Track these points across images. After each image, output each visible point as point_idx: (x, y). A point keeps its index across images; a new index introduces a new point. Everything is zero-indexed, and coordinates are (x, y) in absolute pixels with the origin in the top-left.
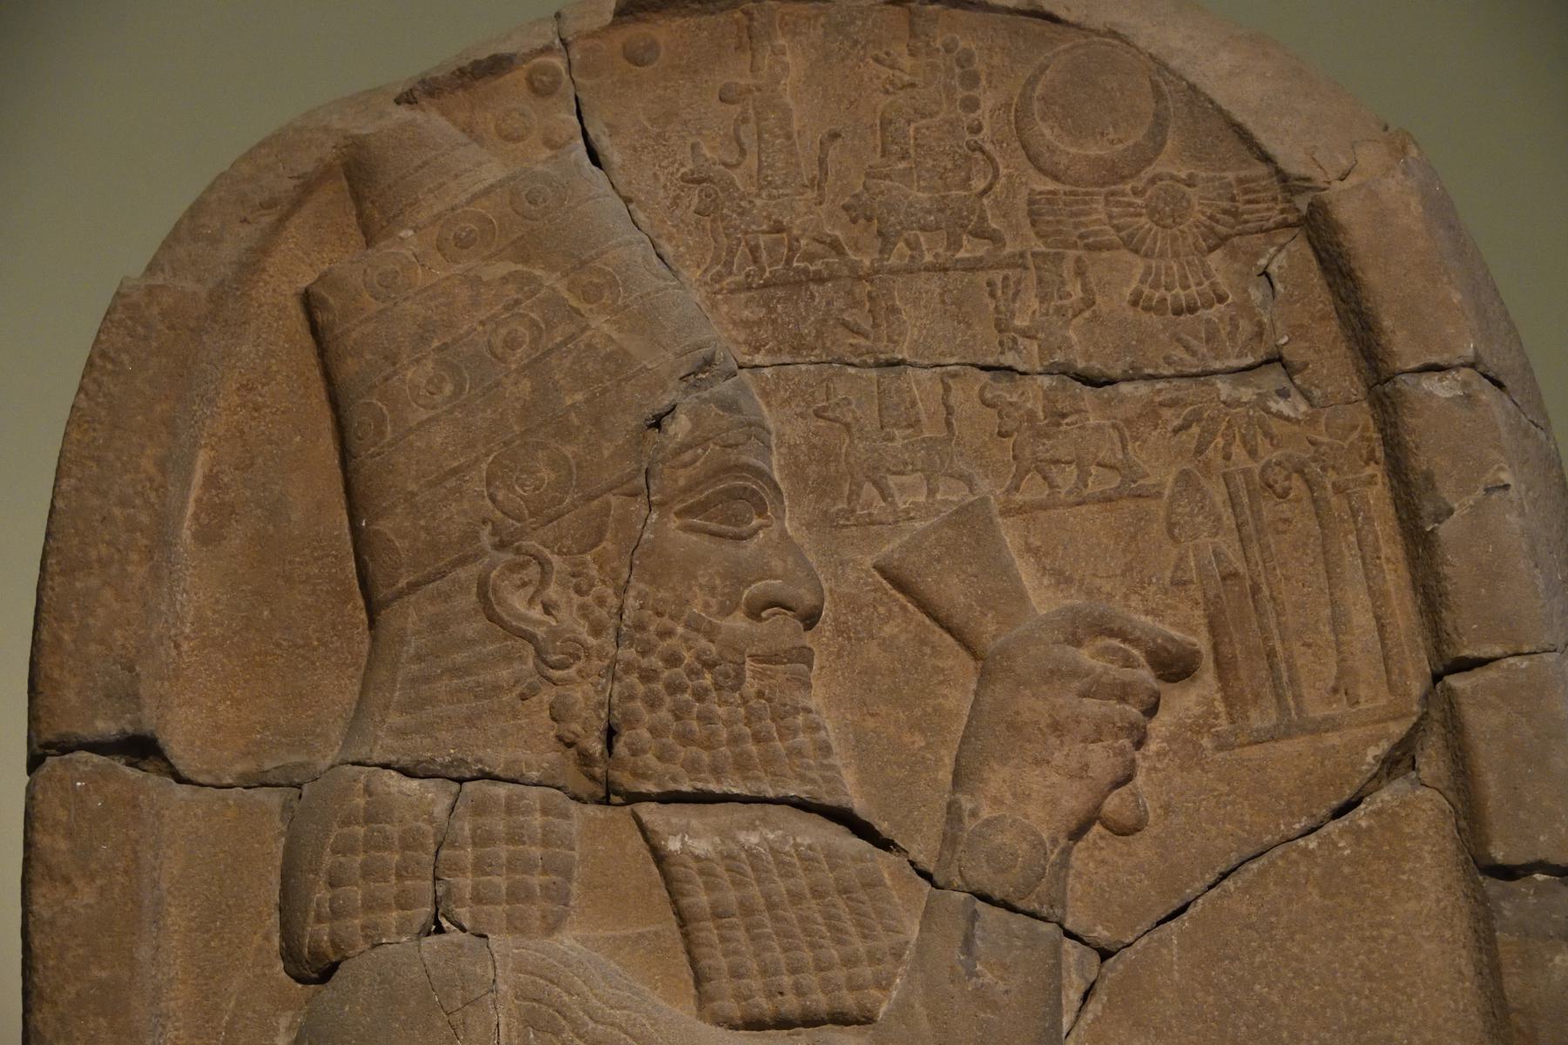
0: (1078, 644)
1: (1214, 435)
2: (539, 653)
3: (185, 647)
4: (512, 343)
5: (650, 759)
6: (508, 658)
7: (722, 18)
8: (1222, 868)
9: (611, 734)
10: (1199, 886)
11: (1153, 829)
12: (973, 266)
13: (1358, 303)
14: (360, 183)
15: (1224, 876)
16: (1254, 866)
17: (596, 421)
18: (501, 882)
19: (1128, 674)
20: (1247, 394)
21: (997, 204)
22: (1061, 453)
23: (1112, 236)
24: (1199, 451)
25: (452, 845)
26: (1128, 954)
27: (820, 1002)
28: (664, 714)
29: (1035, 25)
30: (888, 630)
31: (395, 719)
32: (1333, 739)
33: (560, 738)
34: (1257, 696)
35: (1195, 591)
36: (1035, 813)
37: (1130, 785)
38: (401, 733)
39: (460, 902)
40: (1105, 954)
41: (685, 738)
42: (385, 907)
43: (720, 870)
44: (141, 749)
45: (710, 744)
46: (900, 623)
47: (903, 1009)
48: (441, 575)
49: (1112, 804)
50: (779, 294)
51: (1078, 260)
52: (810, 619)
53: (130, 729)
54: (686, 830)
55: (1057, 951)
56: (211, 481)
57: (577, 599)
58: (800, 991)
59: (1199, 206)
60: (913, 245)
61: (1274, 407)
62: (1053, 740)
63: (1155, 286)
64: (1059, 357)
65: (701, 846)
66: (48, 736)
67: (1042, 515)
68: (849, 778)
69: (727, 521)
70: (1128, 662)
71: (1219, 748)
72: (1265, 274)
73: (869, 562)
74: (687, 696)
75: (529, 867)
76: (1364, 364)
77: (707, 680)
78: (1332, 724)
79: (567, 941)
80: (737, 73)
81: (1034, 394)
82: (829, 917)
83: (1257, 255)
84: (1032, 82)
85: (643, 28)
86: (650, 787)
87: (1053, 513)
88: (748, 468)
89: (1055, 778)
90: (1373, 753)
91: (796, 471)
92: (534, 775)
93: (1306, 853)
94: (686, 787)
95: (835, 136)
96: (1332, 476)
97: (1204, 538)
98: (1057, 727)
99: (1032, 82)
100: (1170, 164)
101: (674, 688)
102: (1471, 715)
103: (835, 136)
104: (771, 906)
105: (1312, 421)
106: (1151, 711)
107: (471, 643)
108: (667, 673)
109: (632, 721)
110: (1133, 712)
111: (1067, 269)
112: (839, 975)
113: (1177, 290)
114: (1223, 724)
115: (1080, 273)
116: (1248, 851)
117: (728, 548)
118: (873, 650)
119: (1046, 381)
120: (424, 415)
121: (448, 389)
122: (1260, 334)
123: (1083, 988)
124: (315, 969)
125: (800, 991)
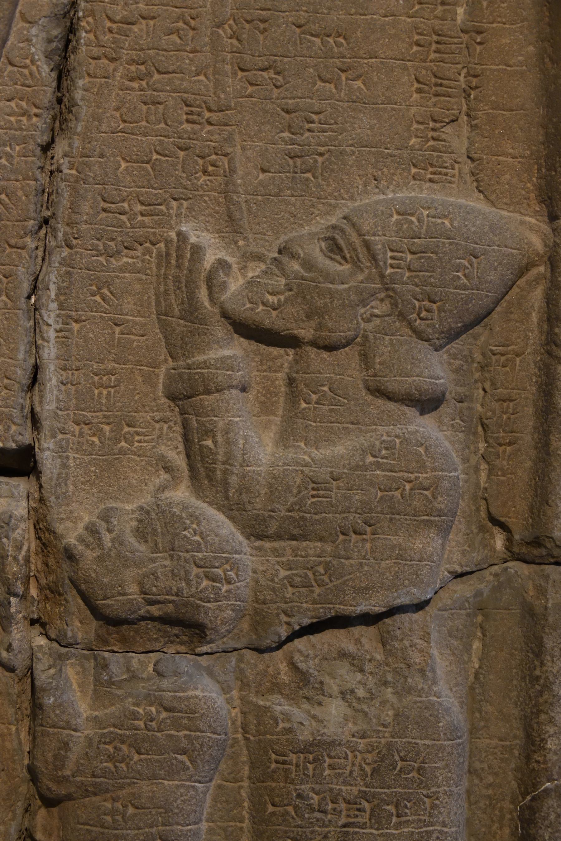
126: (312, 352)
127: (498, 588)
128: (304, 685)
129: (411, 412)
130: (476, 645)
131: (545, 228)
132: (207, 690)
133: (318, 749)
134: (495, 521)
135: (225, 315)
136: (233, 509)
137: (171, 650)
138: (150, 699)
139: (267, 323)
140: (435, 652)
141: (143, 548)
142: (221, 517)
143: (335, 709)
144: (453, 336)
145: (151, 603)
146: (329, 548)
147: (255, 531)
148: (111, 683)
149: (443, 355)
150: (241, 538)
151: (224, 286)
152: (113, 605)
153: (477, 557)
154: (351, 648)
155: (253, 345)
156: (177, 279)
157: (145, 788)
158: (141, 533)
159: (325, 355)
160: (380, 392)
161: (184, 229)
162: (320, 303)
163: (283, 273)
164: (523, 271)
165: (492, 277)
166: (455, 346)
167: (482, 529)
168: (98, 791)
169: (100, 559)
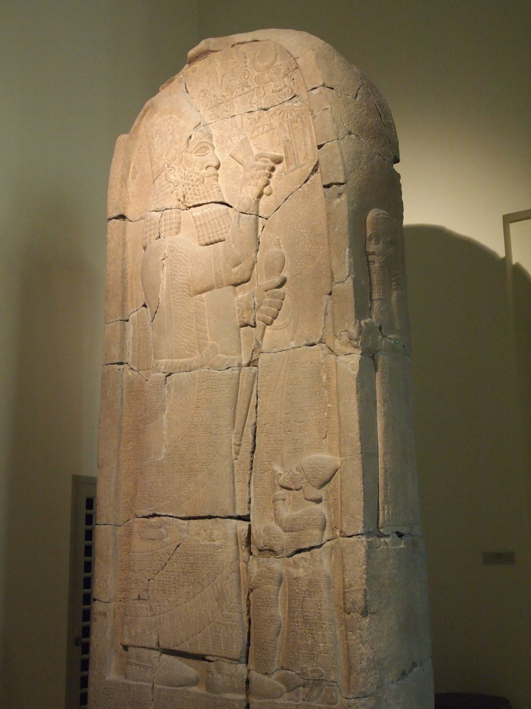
0: (257, 160)
1: (285, 114)
3: (130, 198)
4: (169, 130)
5: (190, 200)
6: (169, 187)
7: (206, 59)
8: (285, 198)
9: (184, 196)
10: (282, 202)
15: (286, 199)
16: (291, 196)
17: (181, 140)
18: (168, 227)
19: (265, 164)
20: (290, 104)
21: (250, 80)
22: (260, 125)
26: (270, 218)
27: (217, 238)
28: (192, 191)
31: (155, 202)
32: (304, 168)
34: (292, 163)
35: (281, 145)
36: (250, 195)
37: (268, 186)
38: (155, 204)
40: (267, 219)
41: (195, 195)
43: (201, 217)
44: (122, 217)
48: (160, 175)
49: (266, 190)
50: (215, 108)
51: (263, 86)
52: (217, 168)
53: (119, 214)
54: (197, 212)
55: (257, 219)
56: (134, 167)
59: (283, 69)
60: (237, 92)
61: (294, 105)
62: (251, 180)
64: (260, 107)
65: (198, 214)
66: (108, 218)
67: (257, 138)
68: (225, 196)
69: (201, 153)
70: (266, 162)
73: (228, 154)
75: (172, 224)
77: (198, 182)
78: (304, 165)
81: (255, 115)
82: (218, 222)
85: (194, 65)
87: (259, 137)
88: (204, 142)
89: (252, 187)
91: (217, 141)
92: (174, 207)
93: (299, 191)
94: (196, 203)
97: (283, 134)
100: (278, 63)
101: (193, 186)
103: (224, 76)
104: (209, 222)
105: (301, 106)
106: (273, 169)
107: (164, 186)
108: (191, 183)
109: (187, 193)
110: (267, 171)
111: (261, 88)
113: (279, 87)
116: (290, 193)
117: (202, 158)
119: (258, 112)
120: (157, 146)
121: (160, 141)
122: (292, 91)
123: (262, 226)
127: (336, 543)
128: (296, 565)
129: (313, 503)
130: (333, 557)
132: (277, 565)
133: (297, 579)
136: (280, 526)
137: (272, 557)
138: (266, 567)
140: (324, 558)
141: (263, 534)
142: (278, 527)
143: (301, 570)
144: (321, 486)
145: (266, 546)
146: (297, 533)
149: (321, 490)
150: (282, 531)
151: (279, 478)
153: (331, 536)
154: (305, 557)
158: (264, 531)
159: (297, 492)
160: (306, 499)
164: (337, 470)
165: (328, 472)
166: (324, 488)
167: (333, 529)
169: (257, 537)
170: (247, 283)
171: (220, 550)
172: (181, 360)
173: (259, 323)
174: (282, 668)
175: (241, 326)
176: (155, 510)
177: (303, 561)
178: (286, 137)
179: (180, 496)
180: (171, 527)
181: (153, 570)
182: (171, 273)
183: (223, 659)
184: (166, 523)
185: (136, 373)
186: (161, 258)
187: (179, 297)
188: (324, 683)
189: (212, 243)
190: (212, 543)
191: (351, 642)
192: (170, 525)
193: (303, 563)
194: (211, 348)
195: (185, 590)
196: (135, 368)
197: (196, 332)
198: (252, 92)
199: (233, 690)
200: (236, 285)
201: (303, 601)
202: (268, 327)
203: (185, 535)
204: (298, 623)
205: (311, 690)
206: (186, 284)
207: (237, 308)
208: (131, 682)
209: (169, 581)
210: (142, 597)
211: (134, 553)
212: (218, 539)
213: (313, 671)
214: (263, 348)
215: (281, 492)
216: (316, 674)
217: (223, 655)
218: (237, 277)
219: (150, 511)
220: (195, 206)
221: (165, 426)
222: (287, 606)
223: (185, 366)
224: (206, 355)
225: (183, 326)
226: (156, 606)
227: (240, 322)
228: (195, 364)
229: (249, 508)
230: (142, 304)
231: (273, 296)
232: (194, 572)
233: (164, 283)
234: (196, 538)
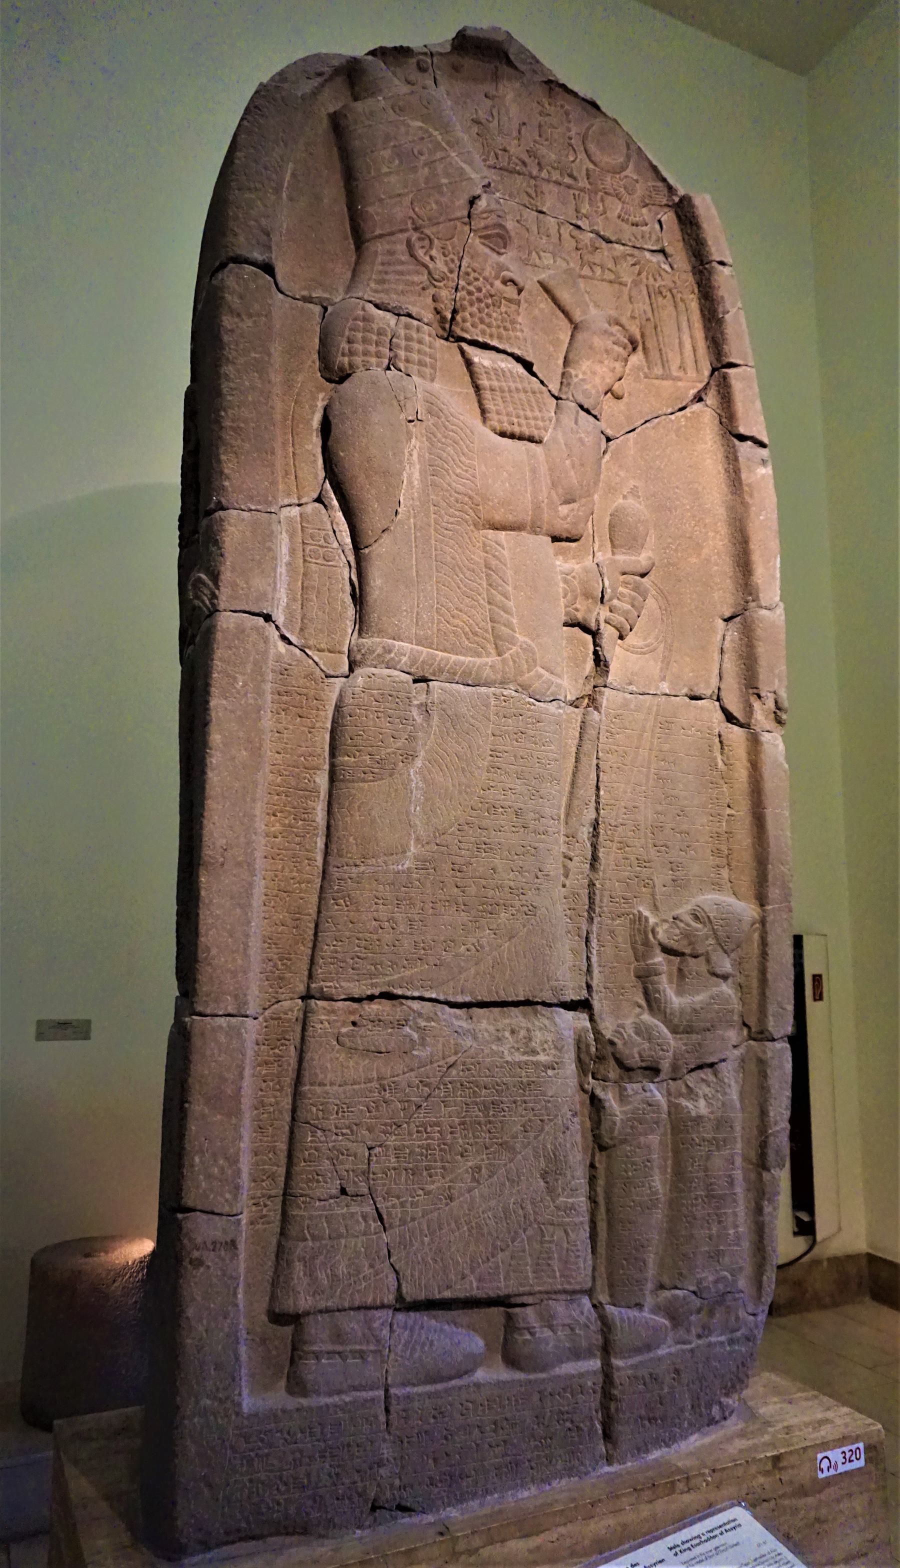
2: (430, 273)
5: (468, 324)
9: (455, 312)
11: (625, 400)
12: (569, 187)
13: (698, 235)
14: (352, 74)
22: (597, 261)
23: (612, 191)
24: (639, 274)
25: (398, 338)
26: (617, 441)
28: (474, 309)
29: (589, 107)
30: (542, 306)
32: (680, 384)
33: (436, 309)
35: (637, 322)
39: (400, 360)
40: (609, 440)
41: (482, 321)
42: (371, 356)
45: (489, 326)
46: (545, 304)
47: (554, 440)
52: (520, 291)
57: (443, 258)
58: (519, 425)
62: (605, 356)
63: (626, 213)
64: (596, 228)
65: (486, 363)
71: (646, 377)
72: (660, 222)
73: (536, 279)
74: (483, 305)
76: (693, 259)
77: (490, 301)
79: (437, 386)
80: (489, 88)
83: (658, 214)
84: (588, 128)
86: (468, 336)
90: (693, 392)
94: (481, 340)
95: (524, 124)
96: (679, 295)
98: (607, 351)
99: (588, 128)
101: (479, 300)
102: (733, 382)
111: (599, 197)
112: (532, 422)
114: (646, 370)
115: (602, 200)
118: (536, 311)
119: (592, 235)
124: (337, 375)
125: (519, 425)
126: (689, 959)
127: (748, 1052)
128: (691, 1093)
131: (759, 910)
133: (699, 1119)
134: (745, 1024)
135: (660, 944)
136: (667, 1022)
139: (675, 947)
147: (674, 1031)
148: (628, 1096)
152: (628, 1062)
155: (666, 956)
156: (639, 930)
157: (642, 1139)
160: (714, 974)
161: (641, 909)
162: (693, 939)
163: (678, 927)
168: (624, 1141)
170: (573, 545)
171: (550, 1072)
172: (454, 657)
173: (608, 633)
174: (662, 1287)
175: (566, 624)
176: (389, 984)
177: (704, 1086)
178: (645, 312)
179: (457, 955)
180: (433, 1024)
181: (385, 1125)
182: (430, 460)
183: (554, 1297)
184: (420, 1015)
185: (298, 651)
186: (402, 416)
187: (452, 520)
188: (729, 1296)
189: (512, 436)
190: (531, 1058)
191: (767, 1219)
192: (429, 1019)
193: (705, 1089)
194: (524, 650)
195: (470, 1164)
196: (293, 639)
197: (488, 607)
198: (582, 194)
199: (577, 1354)
200: (555, 539)
201: (708, 1158)
202: (619, 641)
203: (468, 1042)
204: (696, 1199)
205: (711, 1313)
206: (470, 497)
207: (562, 585)
208: (325, 1400)
209: (428, 1147)
210: (350, 1189)
211: (321, 1084)
212: (544, 1050)
213: (716, 1282)
214: (610, 678)
215: (659, 958)
216: (721, 1286)
217: (559, 1287)
218: (566, 526)
219: (372, 985)
220: (474, 343)
221: (417, 795)
222: (669, 1170)
223: (467, 673)
224: (514, 662)
225: (457, 584)
226: (393, 1206)
227: (567, 614)
228: (487, 673)
229: (589, 987)
230: (315, 496)
231: (637, 588)
232: (490, 1122)
233: (413, 474)
234: (494, 1047)
